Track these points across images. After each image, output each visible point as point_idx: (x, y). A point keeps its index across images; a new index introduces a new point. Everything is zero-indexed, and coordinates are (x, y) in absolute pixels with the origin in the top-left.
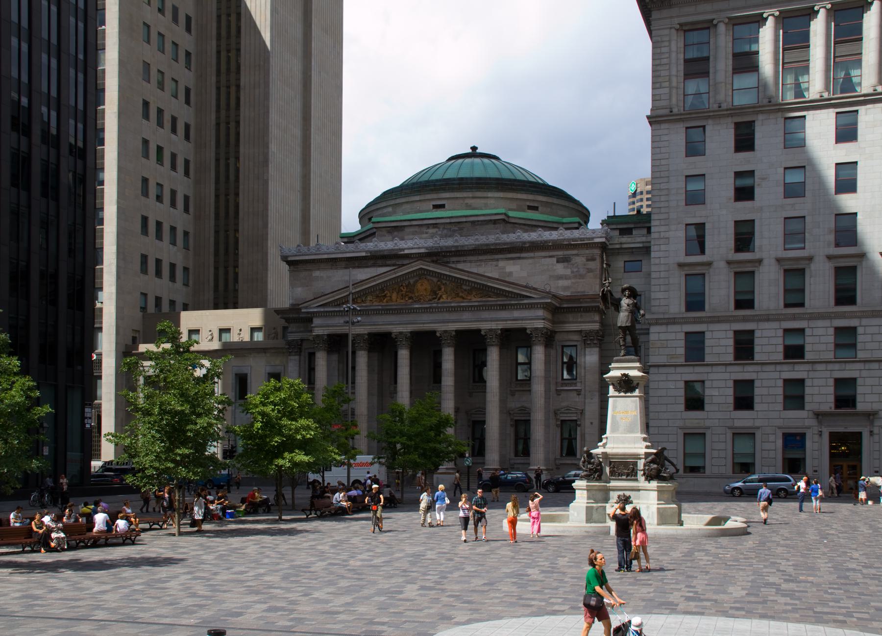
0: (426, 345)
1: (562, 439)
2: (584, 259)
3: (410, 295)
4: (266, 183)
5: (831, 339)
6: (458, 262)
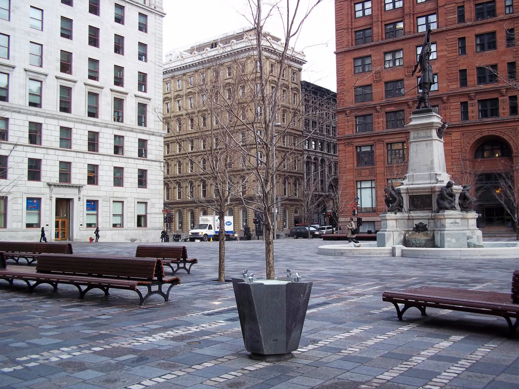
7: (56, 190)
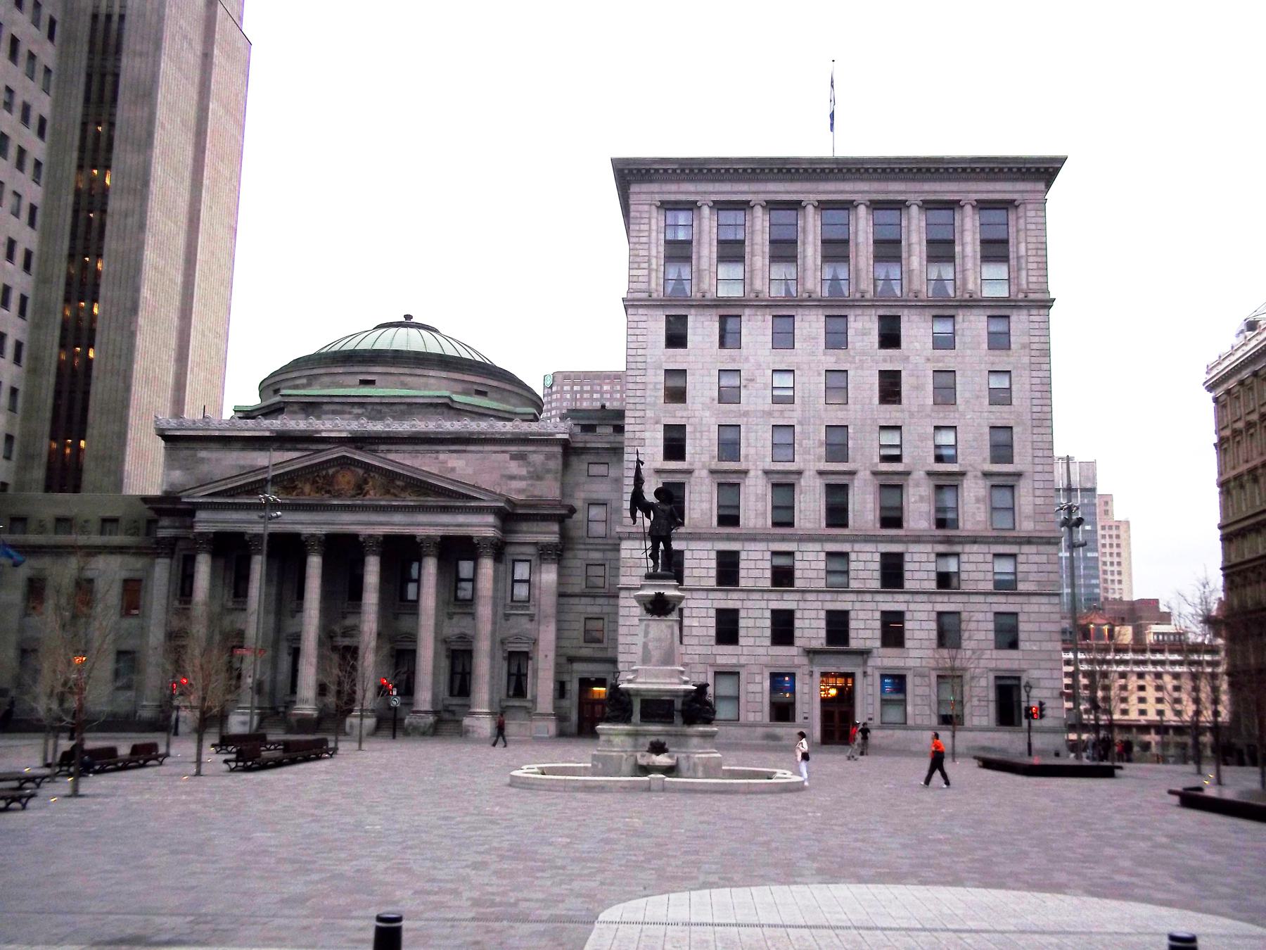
0: (344, 554)
1: (510, 675)
2: (542, 457)
4: (132, 335)
5: (822, 565)
6: (389, 451)
7: (818, 658)
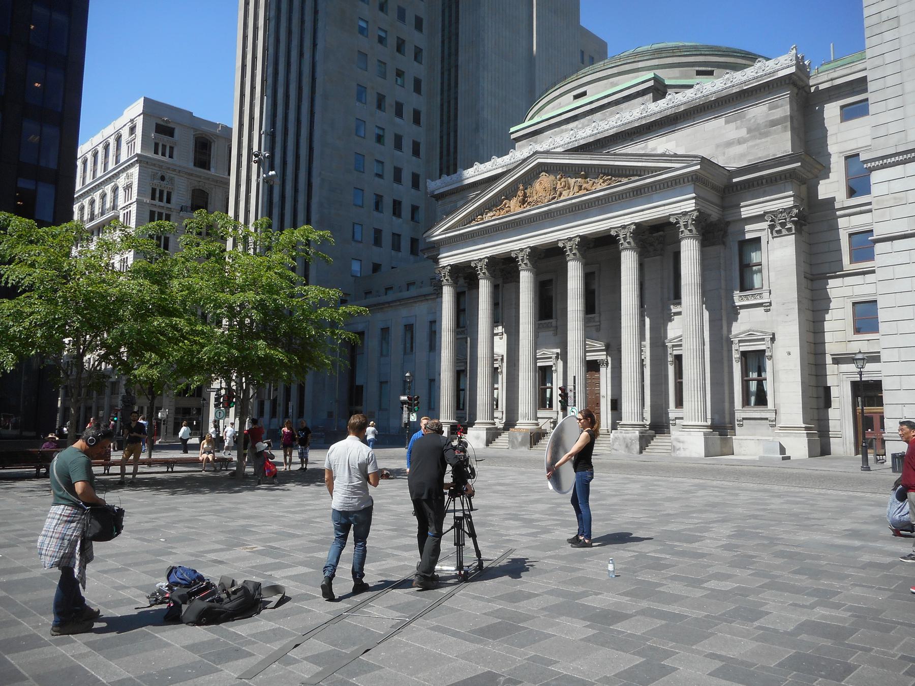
3: (529, 200)
